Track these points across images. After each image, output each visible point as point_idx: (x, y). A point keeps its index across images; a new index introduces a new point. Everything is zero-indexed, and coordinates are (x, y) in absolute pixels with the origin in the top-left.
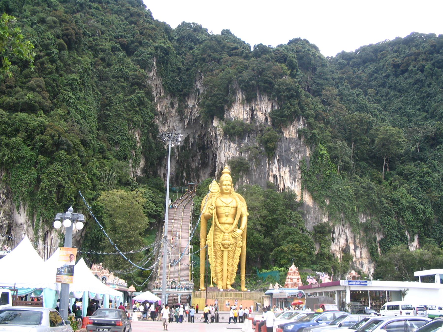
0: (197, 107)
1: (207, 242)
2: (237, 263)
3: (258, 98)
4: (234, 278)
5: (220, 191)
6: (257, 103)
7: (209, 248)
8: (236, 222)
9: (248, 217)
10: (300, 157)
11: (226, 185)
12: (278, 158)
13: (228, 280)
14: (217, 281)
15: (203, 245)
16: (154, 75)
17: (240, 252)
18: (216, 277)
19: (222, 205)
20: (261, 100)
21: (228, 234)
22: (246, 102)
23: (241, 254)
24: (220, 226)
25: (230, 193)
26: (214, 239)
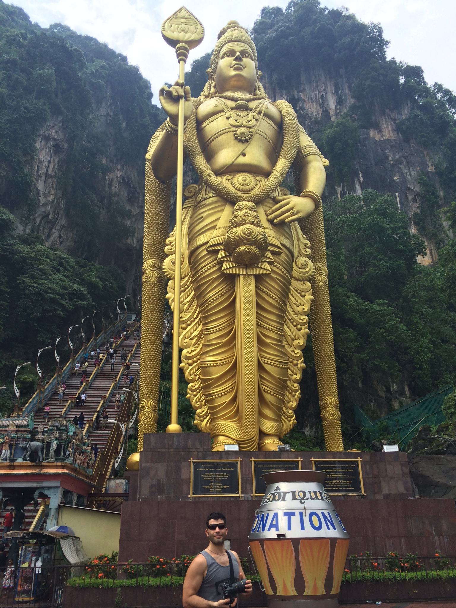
0: (190, 173)
1: (167, 262)
2: (302, 342)
3: (303, 78)
4: (294, 404)
5: (213, 90)
6: (302, 89)
7: (170, 283)
8: (282, 164)
9: (325, 167)
10: (413, 173)
11: (231, 53)
12: (362, 179)
13: (268, 412)
14: (212, 420)
15: (153, 280)
16: (108, 114)
17: (309, 297)
18: (209, 400)
19: (219, 108)
20: (310, 82)
21: (250, 204)
22: (277, 90)
23: (315, 305)
24: (216, 180)
25: (250, 88)
26: (191, 240)
